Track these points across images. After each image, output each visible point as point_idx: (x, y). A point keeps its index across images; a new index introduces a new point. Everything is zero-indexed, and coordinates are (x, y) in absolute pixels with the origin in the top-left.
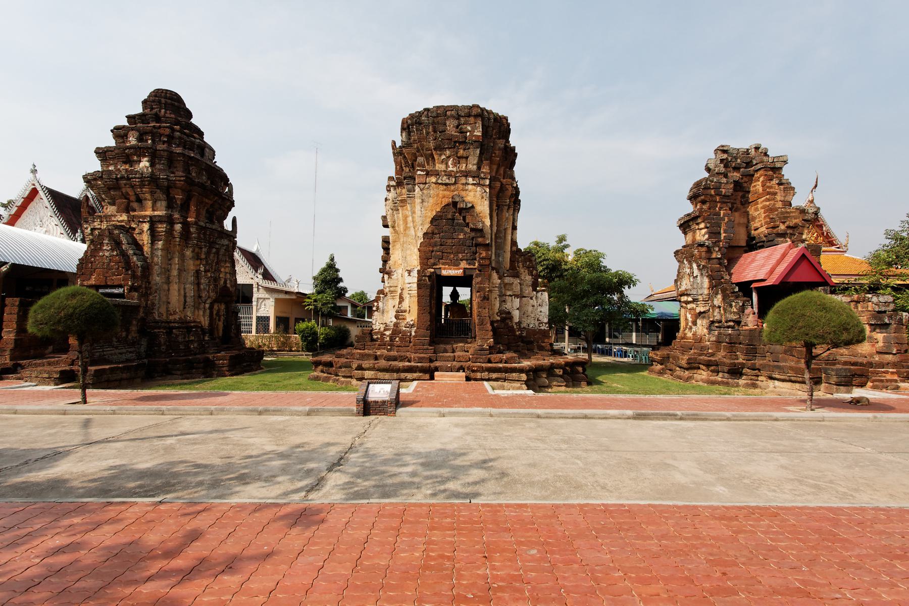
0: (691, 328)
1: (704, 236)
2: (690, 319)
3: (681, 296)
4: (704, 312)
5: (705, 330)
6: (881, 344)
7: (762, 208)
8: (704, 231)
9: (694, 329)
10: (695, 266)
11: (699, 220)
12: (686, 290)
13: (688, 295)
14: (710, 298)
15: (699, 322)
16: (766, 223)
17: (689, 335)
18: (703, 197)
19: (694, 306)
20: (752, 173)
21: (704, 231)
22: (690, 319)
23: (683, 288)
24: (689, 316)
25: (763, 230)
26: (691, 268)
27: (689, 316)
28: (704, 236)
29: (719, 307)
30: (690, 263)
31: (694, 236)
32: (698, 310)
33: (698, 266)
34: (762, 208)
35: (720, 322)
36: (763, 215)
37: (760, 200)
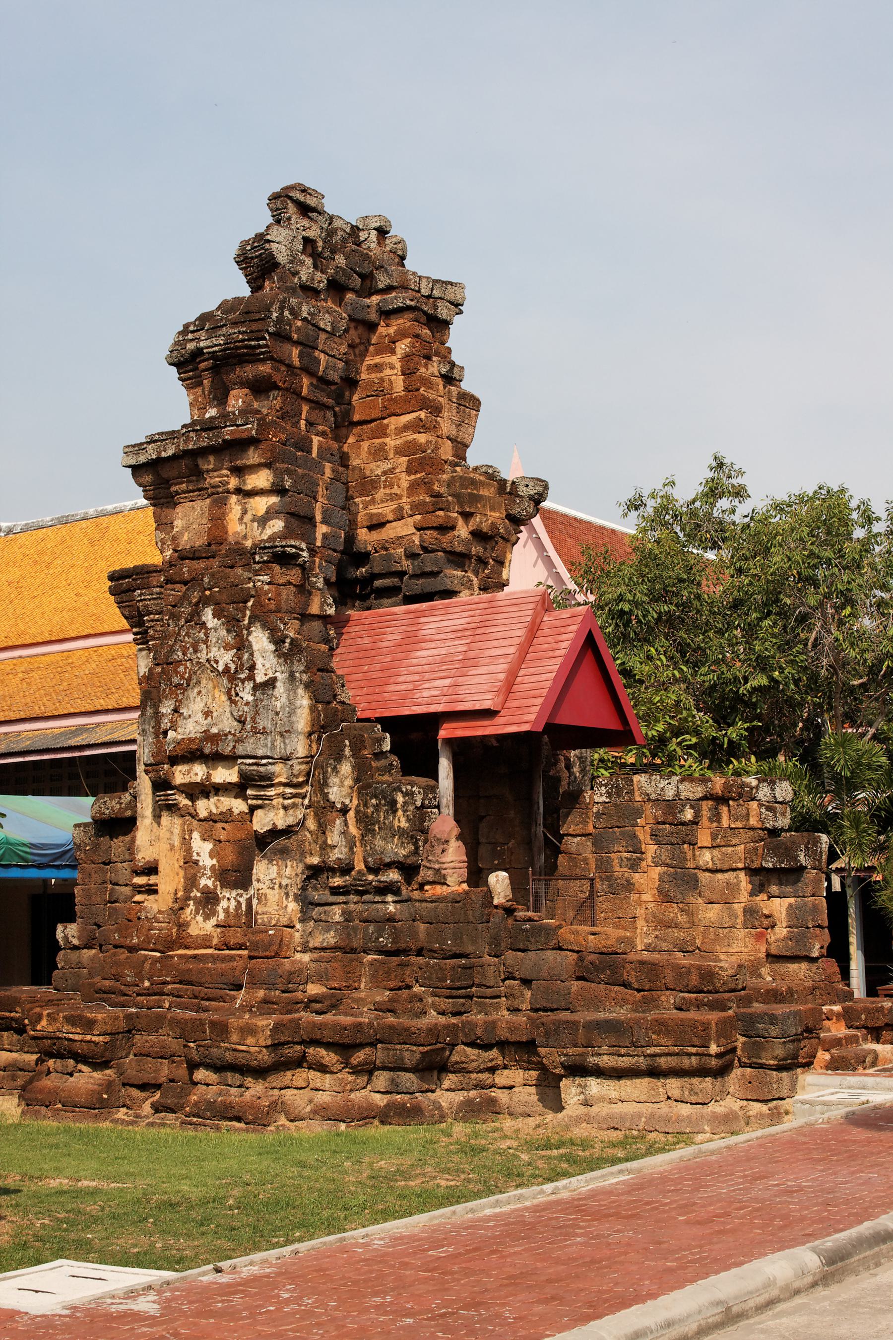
0: (209, 900)
1: (263, 521)
2: (207, 862)
3: (174, 760)
4: (288, 831)
5: (293, 906)
7: (399, 452)
8: (261, 504)
9: (229, 901)
10: (260, 640)
11: (253, 457)
12: (208, 737)
13: (216, 759)
14: (316, 775)
15: (264, 871)
16: (417, 508)
17: (201, 926)
18: (265, 369)
19: (239, 806)
20: (373, 316)
21: (261, 504)
22: (207, 862)
23: (191, 727)
24: (202, 849)
25: (405, 529)
26: (241, 645)
27: (202, 849)
28: (263, 521)
29: (344, 811)
30: (233, 623)
31: (218, 520)
32: (262, 822)
33: (277, 640)
34: (399, 452)
35: (346, 869)
36: (405, 480)
37: (394, 423)
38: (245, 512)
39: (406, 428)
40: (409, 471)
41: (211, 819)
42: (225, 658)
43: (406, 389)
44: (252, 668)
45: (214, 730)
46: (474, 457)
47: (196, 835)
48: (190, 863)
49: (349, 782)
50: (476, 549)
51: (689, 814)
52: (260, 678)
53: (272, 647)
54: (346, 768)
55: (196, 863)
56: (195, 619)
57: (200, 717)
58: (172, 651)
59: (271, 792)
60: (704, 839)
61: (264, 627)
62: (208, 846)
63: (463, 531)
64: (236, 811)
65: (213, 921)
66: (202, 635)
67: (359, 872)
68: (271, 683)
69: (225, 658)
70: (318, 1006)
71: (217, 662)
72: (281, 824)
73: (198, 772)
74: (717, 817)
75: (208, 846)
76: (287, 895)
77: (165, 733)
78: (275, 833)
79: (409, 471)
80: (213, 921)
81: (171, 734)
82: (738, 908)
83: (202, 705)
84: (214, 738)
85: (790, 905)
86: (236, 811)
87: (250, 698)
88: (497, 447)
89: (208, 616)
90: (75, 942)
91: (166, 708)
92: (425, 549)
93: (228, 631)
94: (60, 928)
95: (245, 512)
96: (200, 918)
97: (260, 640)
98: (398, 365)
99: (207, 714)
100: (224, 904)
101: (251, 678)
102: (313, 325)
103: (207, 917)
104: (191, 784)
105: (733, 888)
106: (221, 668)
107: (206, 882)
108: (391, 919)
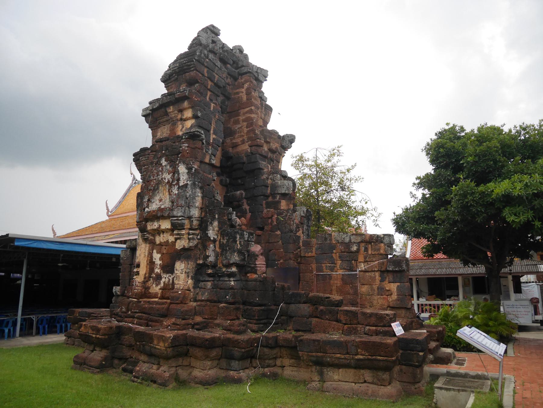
0: (158, 278)
2: (158, 262)
5: (190, 281)
6: (395, 297)
7: (244, 121)
9: (166, 278)
10: (182, 169)
11: (186, 104)
12: (160, 209)
13: (163, 218)
14: (203, 225)
15: (180, 266)
17: (156, 289)
18: (193, 74)
19: (171, 239)
20: (237, 75)
22: (158, 262)
23: (154, 206)
24: (157, 257)
26: (175, 172)
27: (157, 257)
29: (214, 241)
31: (173, 130)
32: (179, 245)
33: (189, 169)
34: (244, 121)
38: (183, 127)
39: (247, 112)
40: (247, 127)
41: (161, 244)
43: (247, 99)
44: (178, 180)
45: (163, 207)
46: (270, 127)
47: (155, 251)
48: (151, 263)
49: (216, 229)
50: (270, 155)
51: (355, 248)
52: (181, 184)
53: (187, 171)
54: (216, 224)
55: (154, 262)
56: (159, 164)
57: (158, 202)
58: (150, 177)
59: (183, 232)
60: (361, 258)
61: (184, 163)
62: (159, 255)
63: (266, 148)
64: (170, 241)
65: (159, 287)
66: (160, 169)
67: (219, 267)
68: (186, 186)
69: (167, 177)
70: (197, 327)
71: (165, 179)
72: (187, 246)
73: (155, 225)
74: (366, 250)
75: (159, 255)
76: (188, 276)
77: (144, 209)
78: (184, 249)
79: (247, 127)
80: (159, 287)
81: (147, 209)
82: (375, 287)
83: (159, 197)
85: (398, 286)
86: (170, 241)
87: (177, 192)
88: (277, 124)
89: (164, 162)
90: (119, 293)
92: (252, 153)
93: (170, 166)
94: (114, 288)
95: (183, 127)
96: (154, 285)
97: (182, 169)
98: (245, 92)
99: (160, 200)
100: (163, 280)
101: (178, 184)
102: (213, 63)
103: (157, 285)
104: (153, 229)
105: (374, 279)
106: (166, 181)
107: (157, 270)
108: (232, 288)
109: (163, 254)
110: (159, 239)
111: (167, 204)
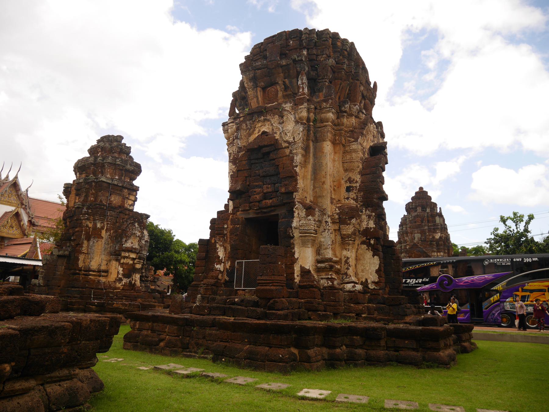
0: (120, 280)
2: (121, 272)
9: (125, 281)
17: (118, 285)
41: (123, 263)
42: (139, 234)
62: (122, 269)
65: (121, 284)
73: (127, 254)
75: (122, 269)
80: (121, 284)
84: (135, 249)
90: (42, 284)
91: (124, 240)
99: (132, 243)
100: (124, 281)
103: (119, 283)
109: (124, 268)
110: (122, 261)
111: (136, 246)
